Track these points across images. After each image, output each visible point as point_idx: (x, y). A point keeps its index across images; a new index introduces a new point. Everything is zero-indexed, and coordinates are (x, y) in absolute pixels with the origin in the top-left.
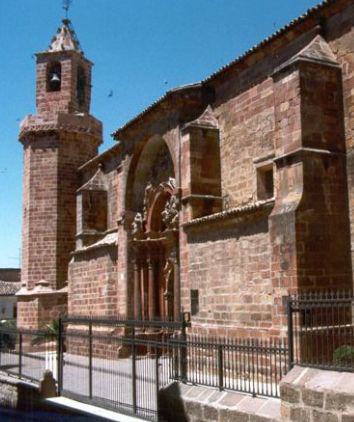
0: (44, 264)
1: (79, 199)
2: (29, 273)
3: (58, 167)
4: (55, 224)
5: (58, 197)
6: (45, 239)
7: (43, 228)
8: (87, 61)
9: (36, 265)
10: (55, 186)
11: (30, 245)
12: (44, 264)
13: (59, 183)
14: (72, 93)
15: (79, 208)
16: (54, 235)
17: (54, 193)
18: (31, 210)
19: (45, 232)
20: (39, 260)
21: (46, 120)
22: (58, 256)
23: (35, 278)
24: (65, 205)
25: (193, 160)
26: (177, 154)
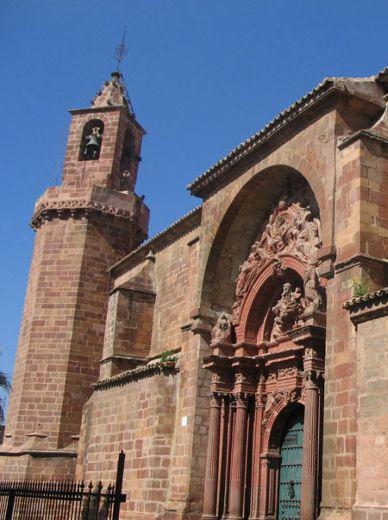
0: (44, 407)
1: (113, 301)
2: (19, 419)
3: (83, 263)
4: (67, 346)
5: (78, 306)
6: (51, 368)
7: (49, 351)
8: (139, 127)
9: (31, 407)
10: (75, 290)
11: (27, 375)
12: (44, 407)
13: (81, 285)
14: (114, 163)
15: (111, 317)
16: (64, 361)
17: (72, 300)
18: (35, 323)
19: (51, 357)
20: (38, 400)
21: (76, 195)
22: (66, 395)
23: (27, 427)
24: (87, 316)
25: (365, 193)
26: (329, 188)
